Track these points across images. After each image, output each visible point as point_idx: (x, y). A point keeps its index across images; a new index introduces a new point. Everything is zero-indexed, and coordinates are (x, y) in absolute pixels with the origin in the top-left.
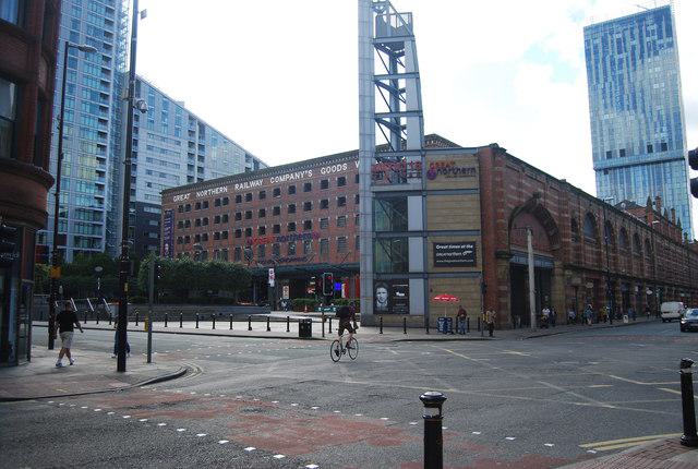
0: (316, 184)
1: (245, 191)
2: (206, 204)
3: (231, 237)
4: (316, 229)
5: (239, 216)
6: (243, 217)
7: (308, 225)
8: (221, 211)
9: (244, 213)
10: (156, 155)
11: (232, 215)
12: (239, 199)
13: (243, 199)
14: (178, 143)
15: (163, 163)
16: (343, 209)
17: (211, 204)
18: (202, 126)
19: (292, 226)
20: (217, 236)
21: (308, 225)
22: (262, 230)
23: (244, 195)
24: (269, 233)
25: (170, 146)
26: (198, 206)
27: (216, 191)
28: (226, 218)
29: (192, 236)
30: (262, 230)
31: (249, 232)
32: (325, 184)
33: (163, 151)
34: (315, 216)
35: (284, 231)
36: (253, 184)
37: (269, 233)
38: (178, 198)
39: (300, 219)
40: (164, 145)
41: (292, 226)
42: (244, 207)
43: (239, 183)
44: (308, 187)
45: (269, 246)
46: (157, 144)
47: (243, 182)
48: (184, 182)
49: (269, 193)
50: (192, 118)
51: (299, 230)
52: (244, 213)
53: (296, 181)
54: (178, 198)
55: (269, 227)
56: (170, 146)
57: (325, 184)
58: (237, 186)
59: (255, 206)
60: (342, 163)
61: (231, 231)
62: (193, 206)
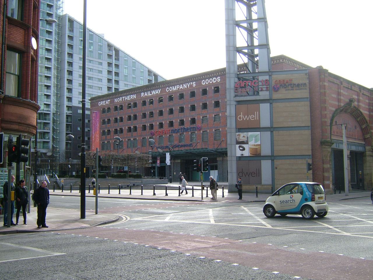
0: (199, 92)
2: (121, 108)
3: (139, 130)
4: (198, 124)
5: (144, 115)
6: (148, 116)
7: (193, 121)
8: (132, 112)
9: (148, 113)
11: (139, 115)
12: (144, 103)
13: (147, 103)
17: (125, 108)
19: (182, 122)
20: (130, 129)
21: (193, 121)
22: (161, 125)
23: (148, 101)
26: (116, 108)
27: (128, 98)
28: (135, 117)
29: (112, 130)
30: (161, 125)
31: (152, 126)
32: (205, 92)
34: (198, 114)
35: (176, 126)
36: (154, 92)
38: (102, 103)
39: (187, 116)
41: (182, 122)
42: (148, 109)
43: (144, 92)
44: (193, 94)
45: (166, 136)
47: (147, 91)
48: (105, 92)
49: (166, 98)
51: (187, 125)
52: (148, 113)
54: (102, 103)
55: (166, 123)
57: (205, 92)
58: (142, 94)
59: (155, 108)
61: (139, 126)
62: (112, 108)
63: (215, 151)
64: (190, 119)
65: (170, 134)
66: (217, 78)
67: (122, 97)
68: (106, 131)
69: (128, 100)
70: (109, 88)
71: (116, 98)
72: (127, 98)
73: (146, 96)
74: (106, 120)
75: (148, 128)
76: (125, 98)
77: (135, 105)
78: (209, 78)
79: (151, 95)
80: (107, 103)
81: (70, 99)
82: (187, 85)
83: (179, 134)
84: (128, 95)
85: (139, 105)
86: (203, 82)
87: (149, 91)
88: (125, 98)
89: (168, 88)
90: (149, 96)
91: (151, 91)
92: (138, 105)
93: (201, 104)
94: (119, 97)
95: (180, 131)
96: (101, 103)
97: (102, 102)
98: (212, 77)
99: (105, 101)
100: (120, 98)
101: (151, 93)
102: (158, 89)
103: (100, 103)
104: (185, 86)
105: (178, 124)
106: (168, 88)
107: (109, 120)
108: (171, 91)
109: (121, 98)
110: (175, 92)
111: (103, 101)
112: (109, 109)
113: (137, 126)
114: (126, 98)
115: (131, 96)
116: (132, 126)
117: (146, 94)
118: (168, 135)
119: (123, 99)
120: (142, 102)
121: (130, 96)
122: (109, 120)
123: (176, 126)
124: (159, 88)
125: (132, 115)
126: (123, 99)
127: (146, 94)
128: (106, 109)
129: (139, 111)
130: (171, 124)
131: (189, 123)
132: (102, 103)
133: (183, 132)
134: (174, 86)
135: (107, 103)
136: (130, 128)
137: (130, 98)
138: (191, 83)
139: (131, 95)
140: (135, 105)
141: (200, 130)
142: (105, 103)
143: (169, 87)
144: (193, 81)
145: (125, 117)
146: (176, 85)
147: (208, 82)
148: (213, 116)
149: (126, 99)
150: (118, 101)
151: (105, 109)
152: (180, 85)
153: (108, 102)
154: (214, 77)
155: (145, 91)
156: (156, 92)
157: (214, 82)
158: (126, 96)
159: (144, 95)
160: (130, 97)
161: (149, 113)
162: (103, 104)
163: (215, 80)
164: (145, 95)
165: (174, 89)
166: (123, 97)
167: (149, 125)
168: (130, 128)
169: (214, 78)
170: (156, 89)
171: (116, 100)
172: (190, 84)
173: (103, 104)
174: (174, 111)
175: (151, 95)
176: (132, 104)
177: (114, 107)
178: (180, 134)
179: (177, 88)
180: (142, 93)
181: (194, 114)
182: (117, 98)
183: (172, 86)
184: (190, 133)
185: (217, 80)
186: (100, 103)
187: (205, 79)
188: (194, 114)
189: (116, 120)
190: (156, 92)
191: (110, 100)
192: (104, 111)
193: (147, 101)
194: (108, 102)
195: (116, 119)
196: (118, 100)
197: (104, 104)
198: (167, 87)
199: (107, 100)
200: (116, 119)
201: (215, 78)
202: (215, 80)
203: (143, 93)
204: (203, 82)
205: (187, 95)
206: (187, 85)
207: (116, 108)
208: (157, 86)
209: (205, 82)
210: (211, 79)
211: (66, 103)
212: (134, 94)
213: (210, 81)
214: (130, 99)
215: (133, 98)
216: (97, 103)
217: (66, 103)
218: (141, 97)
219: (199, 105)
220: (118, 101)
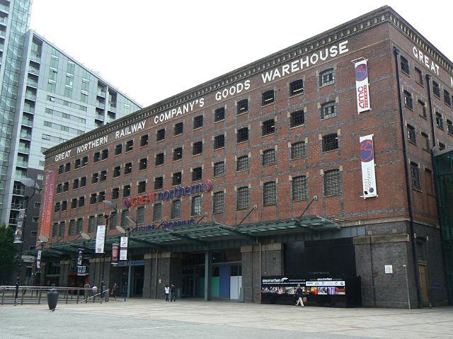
0: (209, 116)
4: (207, 179)
5: (117, 172)
6: (122, 171)
7: (198, 173)
8: (98, 168)
16: (244, 143)
22: (142, 186)
23: (124, 144)
24: (150, 190)
27: (95, 144)
31: (127, 190)
32: (220, 113)
33: (66, 116)
34: (206, 161)
35: (168, 186)
36: (135, 128)
37: (150, 190)
39: (186, 166)
43: (119, 129)
45: (149, 207)
46: (58, 107)
51: (187, 182)
52: (123, 166)
53: (185, 116)
54: (59, 157)
55: (150, 181)
59: (135, 157)
60: (242, 81)
61: (109, 191)
62: (73, 163)
63: (235, 231)
64: (191, 171)
65: (157, 202)
66: (243, 83)
68: (61, 203)
75: (121, 193)
77: (106, 153)
78: (228, 86)
82: (189, 106)
83: (171, 202)
85: (111, 154)
86: (218, 95)
89: (157, 117)
92: (109, 154)
93: (213, 139)
94: (83, 144)
95: (174, 195)
98: (234, 84)
101: (130, 130)
102: (140, 121)
104: (186, 108)
105: (171, 181)
106: (157, 117)
108: (162, 121)
110: (169, 122)
112: (68, 165)
117: (123, 134)
118: (153, 205)
123: (168, 186)
127: (123, 134)
128: (65, 165)
129: (108, 165)
130: (159, 182)
131: (191, 178)
133: (179, 197)
134: (167, 110)
135: (67, 155)
138: (197, 101)
139: (101, 137)
141: (209, 191)
142: (64, 155)
143: (158, 114)
144: (199, 98)
145: (89, 177)
146: (172, 108)
147: (230, 91)
148: (236, 159)
152: (176, 107)
154: (237, 82)
157: (238, 92)
159: (119, 135)
163: (240, 89)
165: (167, 116)
166: (90, 143)
167: (123, 188)
169: (238, 85)
170: (138, 122)
171: (79, 150)
172: (195, 103)
174: (165, 158)
176: (101, 152)
178: (174, 202)
179: (173, 113)
181: (200, 161)
182: (81, 145)
183: (163, 112)
184: (191, 198)
185: (244, 86)
187: (221, 89)
188: (200, 161)
195: (77, 181)
198: (155, 115)
199: (68, 150)
200: (77, 181)
201: (240, 84)
202: (240, 87)
204: (218, 95)
205: (189, 124)
206: (190, 108)
208: (141, 115)
209: (222, 95)
210: (233, 87)
211: (16, 162)
213: (230, 91)
217: (16, 162)
219: (208, 141)
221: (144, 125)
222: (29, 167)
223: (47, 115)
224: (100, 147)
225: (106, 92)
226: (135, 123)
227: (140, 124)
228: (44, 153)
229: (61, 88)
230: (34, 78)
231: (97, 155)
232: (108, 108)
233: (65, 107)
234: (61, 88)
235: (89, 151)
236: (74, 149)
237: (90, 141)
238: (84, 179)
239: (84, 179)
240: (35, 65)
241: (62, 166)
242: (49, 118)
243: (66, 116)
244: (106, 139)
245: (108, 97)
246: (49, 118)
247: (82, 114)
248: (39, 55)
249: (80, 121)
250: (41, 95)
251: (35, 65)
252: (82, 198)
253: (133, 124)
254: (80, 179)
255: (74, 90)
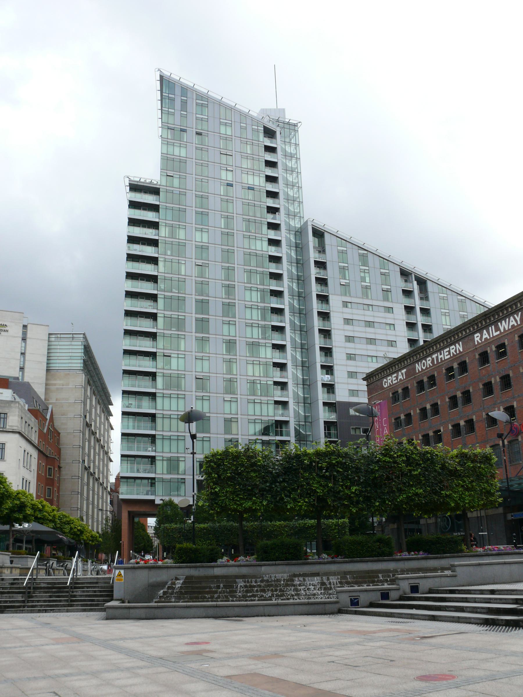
1: (495, 339)
5: (488, 388)
10: (359, 331)
12: (484, 358)
13: (492, 357)
14: (389, 310)
15: (371, 341)
17: (440, 378)
18: (422, 282)
25: (379, 316)
27: (445, 355)
28: (467, 396)
33: (370, 324)
36: (504, 326)
38: (390, 381)
40: (369, 315)
43: (480, 331)
47: (486, 327)
50: (405, 274)
52: (496, 380)
54: (390, 381)
56: (379, 316)
58: (477, 337)
62: (413, 386)
67: (430, 355)
69: (445, 360)
70: (412, 342)
71: (417, 362)
72: (442, 356)
73: (486, 339)
74: (403, 417)
76: (437, 357)
77: (463, 367)
79: (498, 333)
80: (400, 377)
81: (330, 388)
84: (443, 349)
85: (473, 366)
87: (491, 325)
88: (437, 357)
90: (493, 337)
91: (495, 323)
92: (469, 367)
94: (425, 358)
96: (389, 381)
97: (390, 377)
99: (395, 375)
100: (428, 359)
101: (497, 329)
102: (512, 314)
103: (385, 382)
107: (408, 416)
109: (430, 358)
111: (391, 374)
112: (406, 390)
113: (474, 417)
114: (440, 357)
115: (451, 347)
116: (461, 419)
117: (485, 335)
119: (433, 359)
120: (477, 357)
121: (448, 349)
122: (408, 416)
124: (516, 312)
125: (459, 394)
126: (433, 359)
127: (485, 335)
128: (400, 391)
132: (389, 381)
135: (400, 377)
136: (456, 427)
137: (450, 354)
139: (451, 345)
140: (463, 367)
145: (443, 402)
149: (441, 359)
150: (424, 368)
151: (398, 392)
153: (402, 374)
155: (482, 329)
156: (511, 324)
158: (440, 350)
159: (481, 339)
160: (449, 351)
161: (498, 379)
162: (392, 381)
164: (484, 337)
166: (434, 356)
168: (456, 427)
170: (508, 316)
171: (418, 367)
173: (392, 381)
175: (498, 333)
176: (455, 366)
177: (415, 385)
180: (476, 335)
182: (420, 360)
186: (385, 382)
189: (454, 400)
190: (511, 324)
191: (405, 370)
192: (395, 397)
193: (491, 349)
194: (402, 375)
195: (423, 410)
196: (424, 366)
197: (394, 382)
199: (400, 370)
203: (478, 334)
207: (421, 385)
211: (322, 396)
212: (457, 341)
214: (449, 356)
215: (456, 351)
216: (379, 383)
217: (322, 396)
218: (476, 345)
220: (424, 368)
221: (518, 319)
222: (337, 400)
223: (347, 327)
224: (454, 358)
225: (412, 282)
226: (504, 318)
227: (512, 318)
228: (364, 379)
229: (356, 288)
230: (322, 281)
231: (450, 369)
232: (417, 303)
233: (367, 313)
234: (356, 288)
235: (436, 366)
236: (410, 367)
237: (436, 352)
238: (435, 406)
239: (435, 406)
240: (321, 265)
241: (395, 393)
242: (349, 331)
243: (370, 324)
244: (459, 347)
245: (415, 287)
246: (349, 331)
247: (389, 318)
248: (322, 249)
249: (388, 327)
250: (335, 301)
251: (321, 265)
252: (437, 432)
253: (500, 320)
254: (428, 407)
255: (373, 287)
